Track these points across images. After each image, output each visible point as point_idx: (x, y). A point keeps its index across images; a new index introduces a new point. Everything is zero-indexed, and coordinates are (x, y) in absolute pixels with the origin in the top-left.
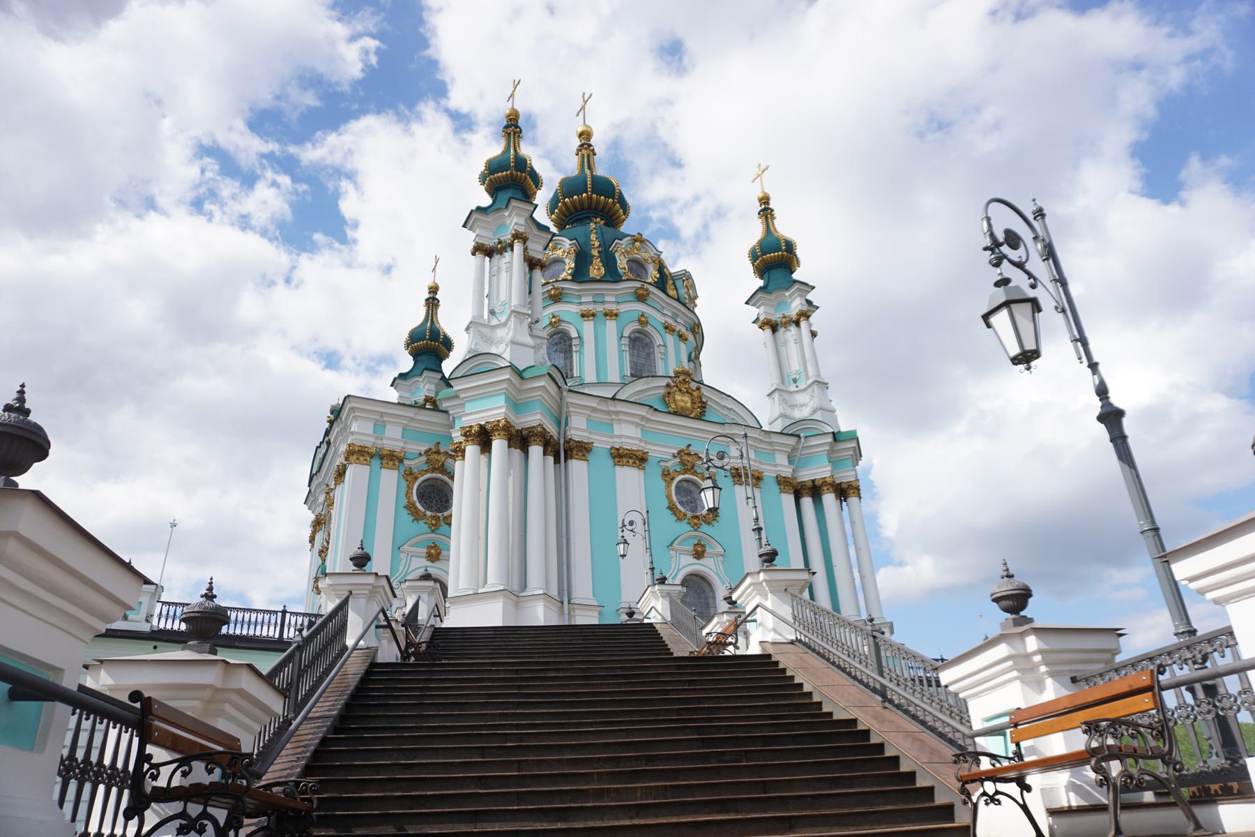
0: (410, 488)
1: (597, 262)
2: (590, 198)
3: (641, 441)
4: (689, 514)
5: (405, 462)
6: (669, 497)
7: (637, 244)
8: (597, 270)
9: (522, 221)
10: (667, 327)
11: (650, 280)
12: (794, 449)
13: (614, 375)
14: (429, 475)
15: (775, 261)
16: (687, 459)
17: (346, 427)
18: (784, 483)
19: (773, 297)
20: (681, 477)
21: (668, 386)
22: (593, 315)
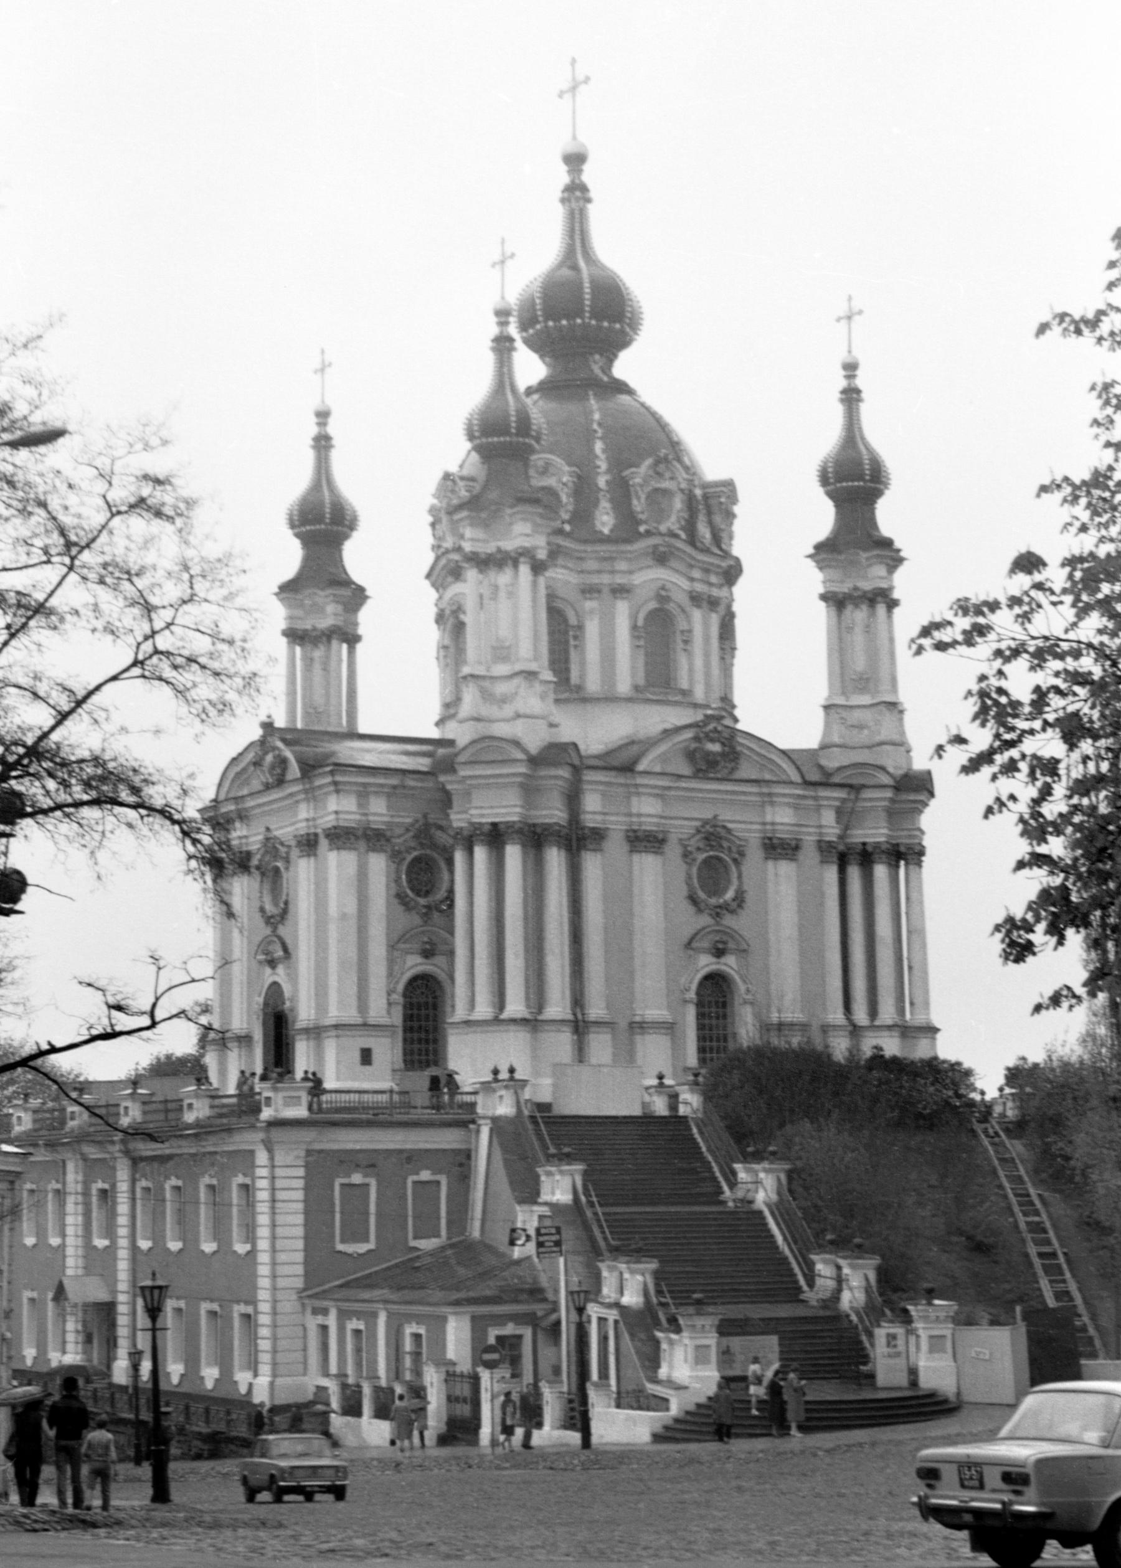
0: (398, 871)
1: (605, 504)
2: (585, 326)
3: (662, 817)
4: (713, 901)
5: (394, 840)
6: (689, 884)
7: (661, 468)
8: (605, 520)
9: (528, 531)
10: (696, 599)
11: (675, 528)
12: (844, 801)
13: (624, 687)
14: (415, 854)
15: (854, 482)
16: (713, 835)
17: (313, 789)
18: (825, 848)
19: (842, 557)
20: (705, 855)
21: (696, 739)
22: (599, 591)
